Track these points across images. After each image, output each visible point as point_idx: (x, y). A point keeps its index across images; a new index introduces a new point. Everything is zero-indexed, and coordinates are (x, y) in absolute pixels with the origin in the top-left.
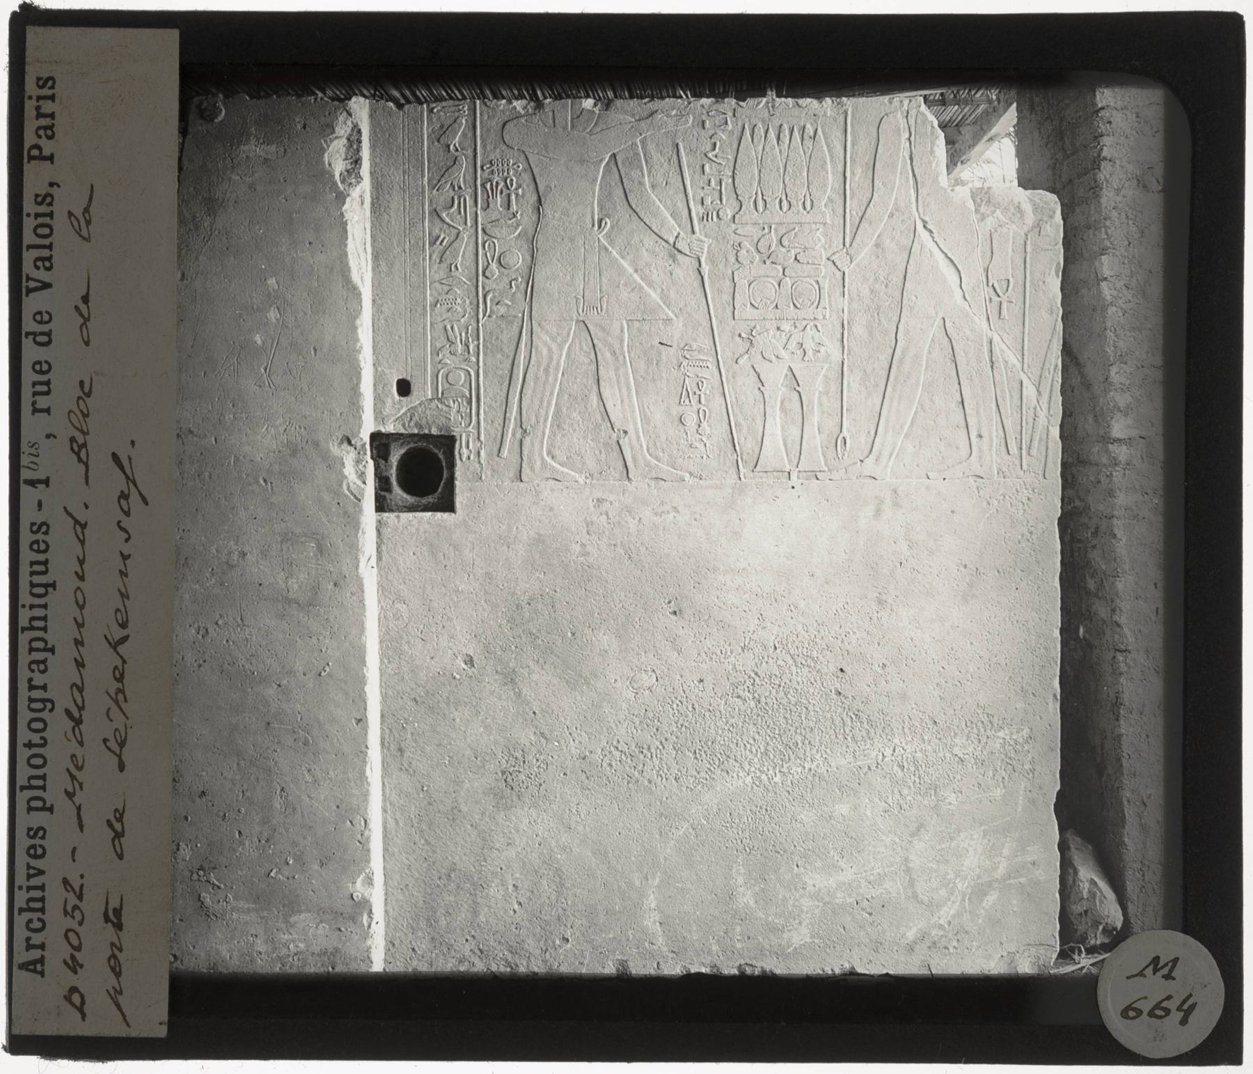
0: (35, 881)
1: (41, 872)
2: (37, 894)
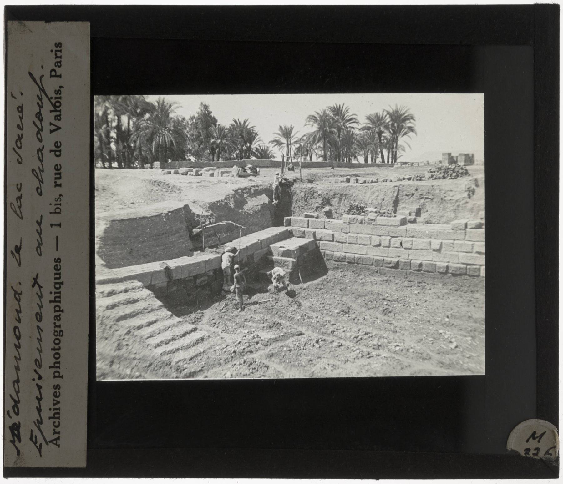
0: (56, 407)
1: (58, 402)
2: (58, 411)
